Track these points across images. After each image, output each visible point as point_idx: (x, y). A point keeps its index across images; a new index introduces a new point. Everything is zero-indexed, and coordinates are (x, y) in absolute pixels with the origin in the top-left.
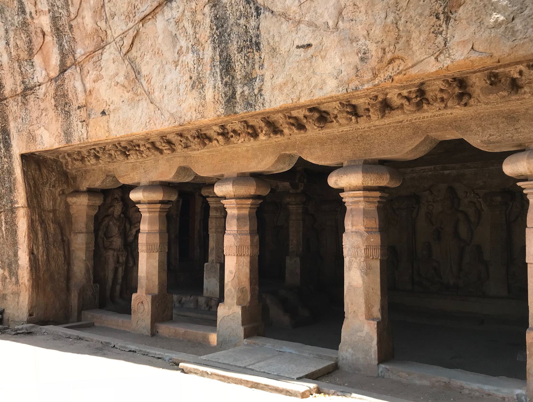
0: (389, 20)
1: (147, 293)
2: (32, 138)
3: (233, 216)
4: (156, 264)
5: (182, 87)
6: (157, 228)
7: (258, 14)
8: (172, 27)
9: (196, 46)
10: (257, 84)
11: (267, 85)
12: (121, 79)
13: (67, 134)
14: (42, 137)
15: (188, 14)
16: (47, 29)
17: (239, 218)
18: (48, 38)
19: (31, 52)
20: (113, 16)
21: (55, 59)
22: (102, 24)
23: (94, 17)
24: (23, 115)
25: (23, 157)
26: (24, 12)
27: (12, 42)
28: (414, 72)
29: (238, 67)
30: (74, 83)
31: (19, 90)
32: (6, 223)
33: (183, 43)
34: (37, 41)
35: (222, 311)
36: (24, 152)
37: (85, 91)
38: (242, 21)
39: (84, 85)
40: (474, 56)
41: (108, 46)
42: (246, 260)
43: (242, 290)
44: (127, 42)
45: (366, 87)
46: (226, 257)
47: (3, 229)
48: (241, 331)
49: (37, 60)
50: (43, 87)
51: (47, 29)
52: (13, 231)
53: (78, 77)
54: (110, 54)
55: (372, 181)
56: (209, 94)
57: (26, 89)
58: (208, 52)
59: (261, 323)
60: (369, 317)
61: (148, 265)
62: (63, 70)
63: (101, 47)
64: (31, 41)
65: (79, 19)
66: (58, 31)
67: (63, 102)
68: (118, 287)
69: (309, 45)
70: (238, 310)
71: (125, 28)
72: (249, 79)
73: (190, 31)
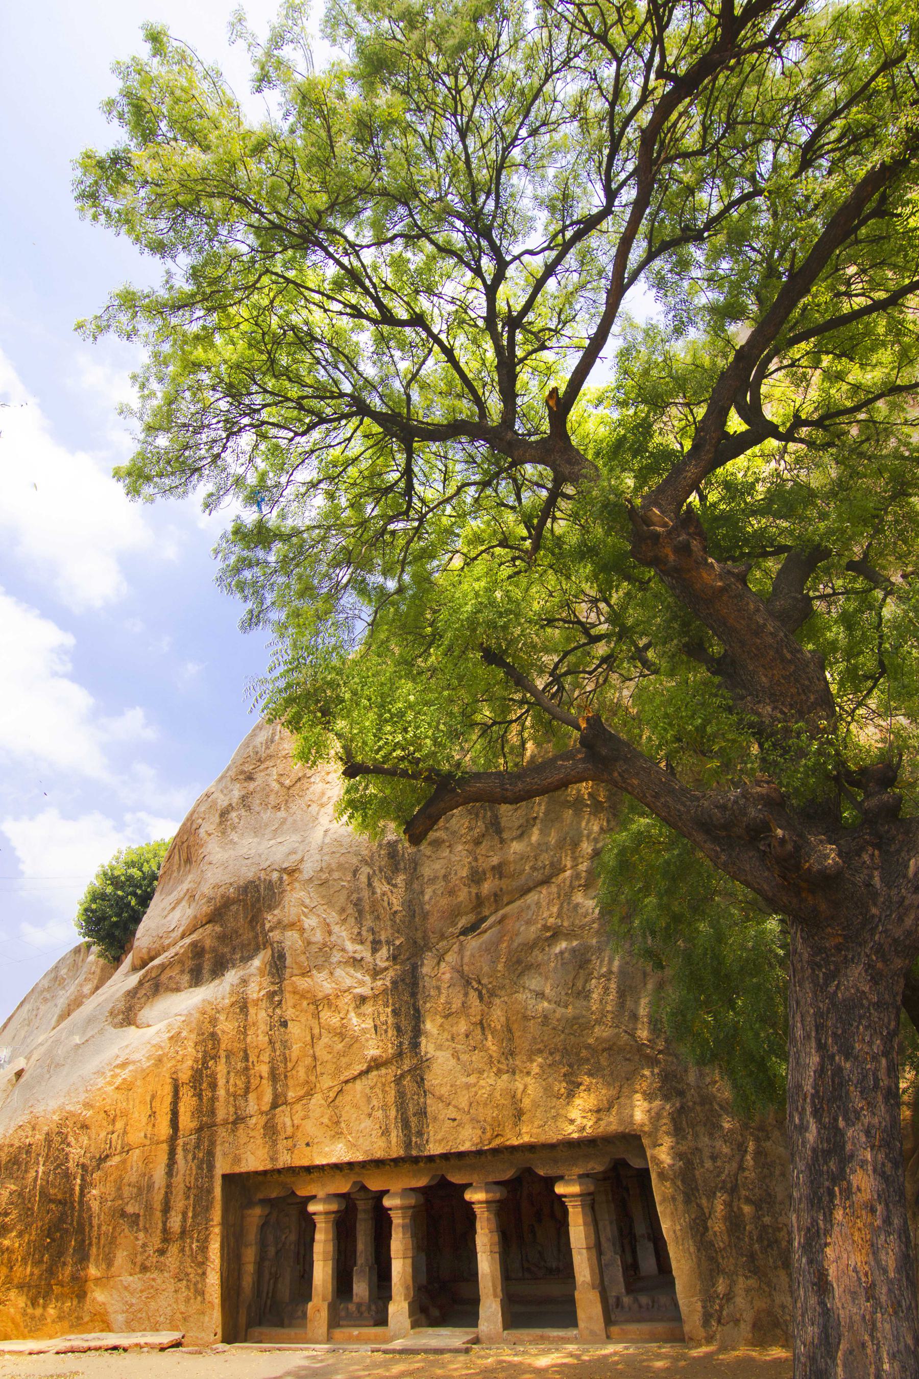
1: (324, 1300)
2: (237, 1160)
3: (398, 1225)
4: (330, 1272)
5: (374, 1133)
6: (331, 1237)
8: (368, 1090)
9: (385, 1107)
11: (432, 1139)
12: (326, 1120)
13: (273, 1159)
15: (379, 1085)
16: (265, 1075)
17: (404, 1226)
18: (264, 1081)
19: (247, 1090)
20: (322, 1074)
21: (268, 1097)
22: (313, 1079)
23: (307, 1073)
24: (231, 1140)
25: (224, 1176)
26: (247, 1060)
27: (232, 1081)
28: (508, 1143)
30: (284, 1118)
31: (231, 1119)
33: (374, 1102)
34: (254, 1082)
35: (392, 1308)
36: (228, 1171)
38: (416, 1097)
42: (409, 1261)
43: (407, 1288)
44: (332, 1094)
48: (407, 1323)
49: (252, 1097)
50: (254, 1120)
51: (265, 1075)
52: (204, 1249)
53: (287, 1113)
54: (317, 1099)
55: (490, 1196)
57: (237, 1119)
58: (393, 1113)
60: (495, 1296)
61: (322, 1273)
62: (275, 1105)
63: (309, 1094)
64: (249, 1082)
65: (294, 1072)
66: (274, 1077)
67: (271, 1130)
68: (269, 1302)
69: (455, 1120)
70: (405, 1305)
71: (331, 1084)
72: (420, 1134)
73: (381, 1096)
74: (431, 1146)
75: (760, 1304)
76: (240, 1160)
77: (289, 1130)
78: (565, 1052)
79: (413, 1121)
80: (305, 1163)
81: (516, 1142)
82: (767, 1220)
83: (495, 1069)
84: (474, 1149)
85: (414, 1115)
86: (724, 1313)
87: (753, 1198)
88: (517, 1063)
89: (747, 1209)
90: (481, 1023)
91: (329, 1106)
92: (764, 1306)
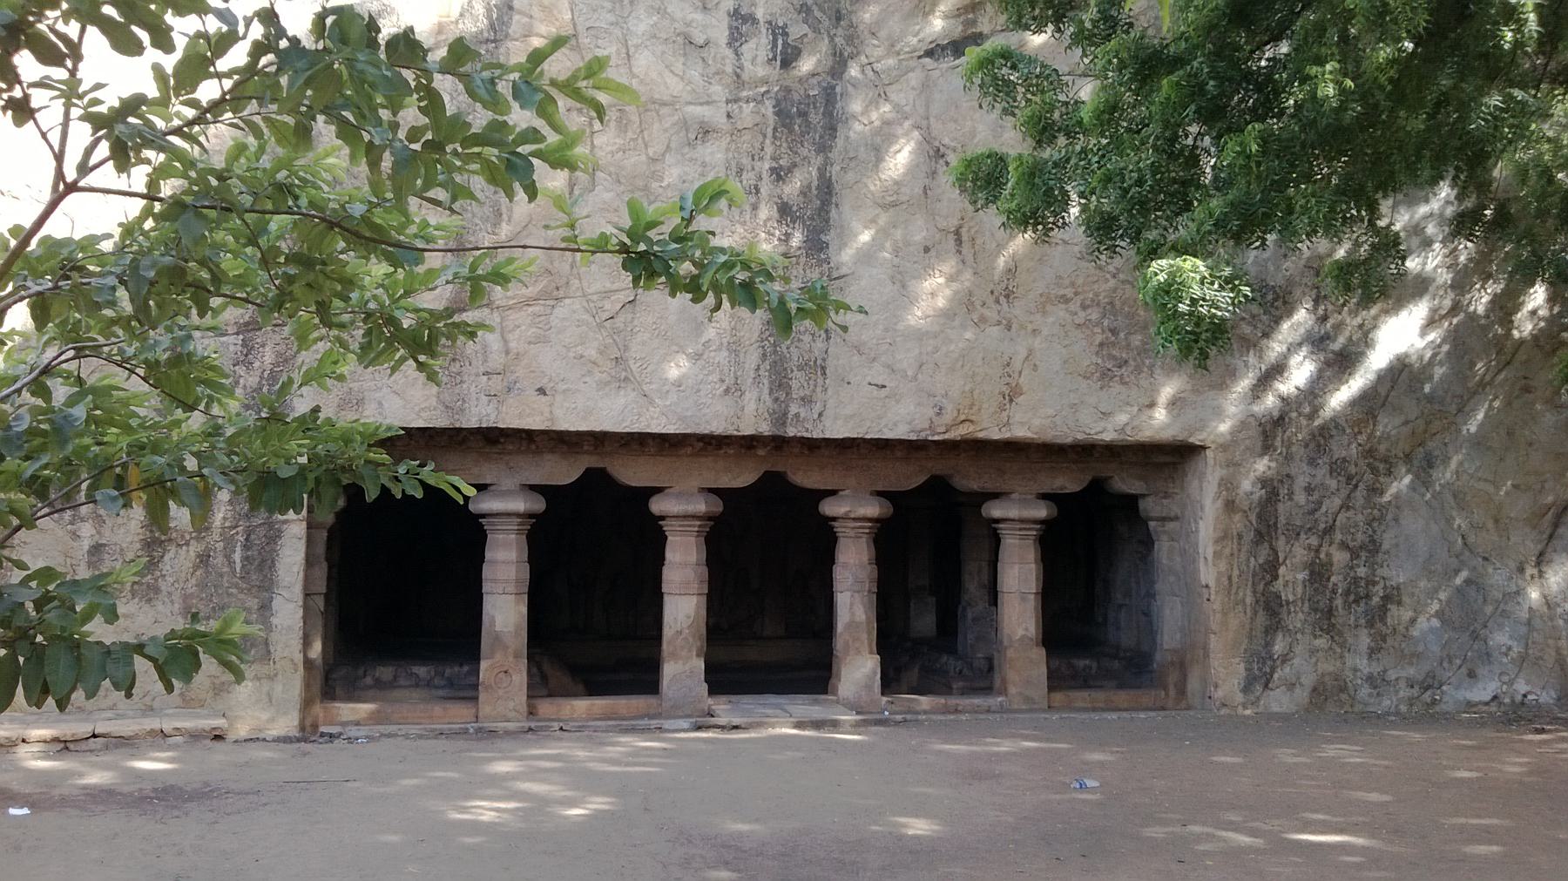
0: (967, 388)
7: (828, 338)
9: (734, 348)
10: (817, 408)
11: (829, 413)
12: (592, 353)
14: (380, 404)
28: (981, 435)
29: (794, 384)
32: (246, 547)
37: (507, 353)
39: (505, 341)
40: (1029, 435)
41: (567, 301)
45: (936, 438)
46: (666, 598)
47: (237, 557)
56: (751, 407)
58: (752, 358)
59: (727, 677)
72: (807, 401)
74: (827, 422)
75: (1328, 667)
76: (360, 402)
77: (497, 360)
78: (1111, 308)
79: (797, 380)
80: (535, 423)
81: (996, 436)
82: (1362, 571)
83: (975, 317)
84: (913, 437)
85: (800, 368)
86: (1276, 676)
87: (1351, 544)
88: (1017, 312)
89: (1340, 557)
90: (957, 233)
91: (600, 326)
92: (1331, 669)
